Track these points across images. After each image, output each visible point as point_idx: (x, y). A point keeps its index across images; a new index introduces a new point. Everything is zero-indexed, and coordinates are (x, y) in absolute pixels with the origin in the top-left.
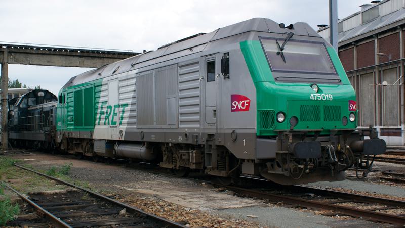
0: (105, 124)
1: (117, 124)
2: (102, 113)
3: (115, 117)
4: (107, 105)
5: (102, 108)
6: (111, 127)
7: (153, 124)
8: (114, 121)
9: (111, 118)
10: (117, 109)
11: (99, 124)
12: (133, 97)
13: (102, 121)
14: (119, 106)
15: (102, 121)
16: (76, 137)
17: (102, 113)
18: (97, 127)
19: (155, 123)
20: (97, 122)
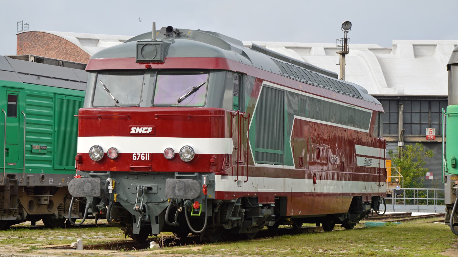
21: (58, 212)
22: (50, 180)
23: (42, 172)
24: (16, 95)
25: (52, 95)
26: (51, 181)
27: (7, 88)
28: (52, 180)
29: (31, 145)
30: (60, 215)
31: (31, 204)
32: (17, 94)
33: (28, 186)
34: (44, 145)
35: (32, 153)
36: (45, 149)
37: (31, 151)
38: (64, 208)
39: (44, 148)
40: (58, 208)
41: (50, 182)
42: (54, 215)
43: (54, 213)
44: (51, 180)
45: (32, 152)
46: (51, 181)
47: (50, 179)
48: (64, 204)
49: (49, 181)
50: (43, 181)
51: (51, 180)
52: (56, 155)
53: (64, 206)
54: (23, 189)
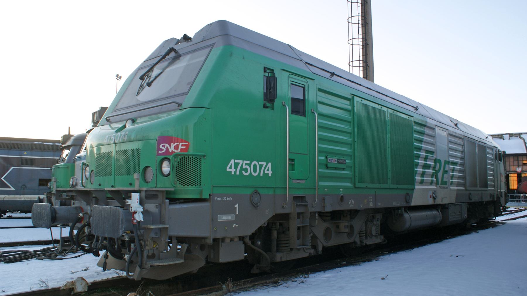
0: (431, 183)
1: (448, 184)
2: (426, 166)
3: (445, 176)
4: (434, 156)
5: (426, 159)
6: (441, 187)
7: (477, 187)
8: (445, 180)
9: (440, 175)
10: (447, 165)
11: (422, 182)
12: (462, 158)
13: (427, 179)
14: (448, 162)
15: (427, 179)
16: (362, 206)
17: (426, 166)
18: (417, 187)
19: (478, 186)
20: (418, 178)
21: (360, 238)
22: (350, 202)
23: (341, 192)
24: (304, 86)
25: (350, 97)
26: (351, 203)
27: (289, 73)
28: (353, 202)
29: (327, 157)
30: (361, 242)
31: (327, 233)
32: (305, 85)
33: (323, 211)
34: (342, 158)
35: (327, 167)
36: (345, 164)
37: (327, 165)
38: (366, 233)
39: (342, 161)
40: (359, 234)
41: (351, 204)
42: (355, 242)
43: (355, 241)
44: (351, 201)
45: (328, 166)
46: (351, 203)
47: (350, 201)
48: (366, 229)
49: (350, 203)
50: (342, 203)
51: (351, 201)
52: (357, 170)
53: (366, 231)
54: (317, 215)
